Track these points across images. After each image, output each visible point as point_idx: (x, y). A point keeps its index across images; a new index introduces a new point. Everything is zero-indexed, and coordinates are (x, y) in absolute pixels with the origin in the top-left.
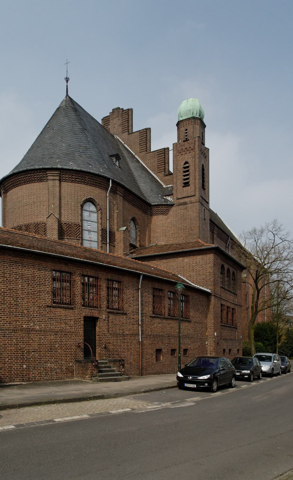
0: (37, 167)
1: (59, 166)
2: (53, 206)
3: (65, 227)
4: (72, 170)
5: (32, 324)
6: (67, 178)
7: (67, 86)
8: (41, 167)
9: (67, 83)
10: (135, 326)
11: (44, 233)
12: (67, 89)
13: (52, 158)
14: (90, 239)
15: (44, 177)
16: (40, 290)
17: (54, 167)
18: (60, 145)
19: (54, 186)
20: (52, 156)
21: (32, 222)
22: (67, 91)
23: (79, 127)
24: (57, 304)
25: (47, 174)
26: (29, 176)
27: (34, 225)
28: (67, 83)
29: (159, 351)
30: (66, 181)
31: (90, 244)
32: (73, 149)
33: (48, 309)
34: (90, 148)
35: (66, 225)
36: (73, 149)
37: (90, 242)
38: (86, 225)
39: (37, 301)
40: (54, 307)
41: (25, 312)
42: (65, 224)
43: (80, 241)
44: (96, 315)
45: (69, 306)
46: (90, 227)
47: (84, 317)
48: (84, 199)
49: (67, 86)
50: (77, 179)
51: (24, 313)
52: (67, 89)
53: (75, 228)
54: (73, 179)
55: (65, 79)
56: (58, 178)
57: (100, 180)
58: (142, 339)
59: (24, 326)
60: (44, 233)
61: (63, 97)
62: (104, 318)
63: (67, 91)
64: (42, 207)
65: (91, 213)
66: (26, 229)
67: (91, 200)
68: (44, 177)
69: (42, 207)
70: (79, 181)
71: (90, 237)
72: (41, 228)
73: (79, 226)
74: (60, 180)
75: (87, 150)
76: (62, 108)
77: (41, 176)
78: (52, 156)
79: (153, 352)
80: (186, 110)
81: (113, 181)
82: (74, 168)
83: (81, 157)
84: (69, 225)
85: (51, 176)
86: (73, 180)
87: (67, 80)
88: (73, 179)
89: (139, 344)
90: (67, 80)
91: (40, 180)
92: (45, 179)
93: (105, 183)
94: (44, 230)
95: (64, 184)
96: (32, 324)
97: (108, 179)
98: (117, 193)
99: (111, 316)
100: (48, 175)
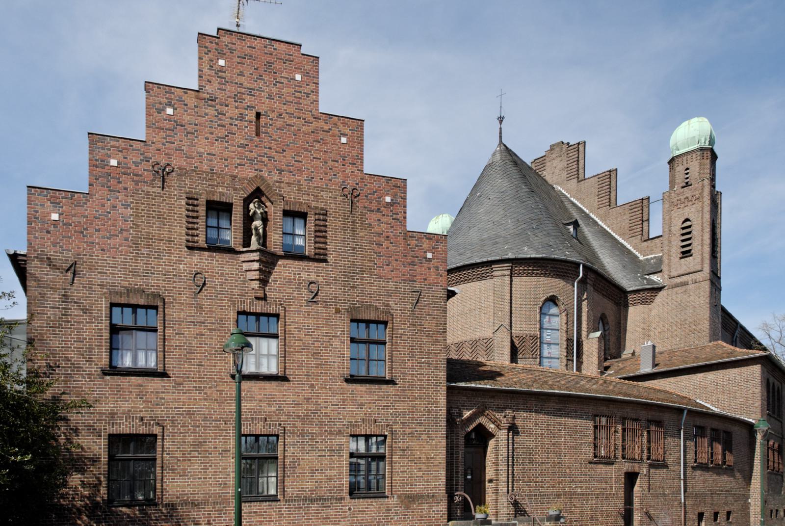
0: (479, 261)
1: (511, 255)
2: (500, 313)
3: (516, 342)
4: (530, 259)
5: (574, 486)
6: (521, 271)
7: (501, 128)
8: (485, 260)
9: (501, 124)
10: (676, 481)
11: (485, 353)
12: (501, 133)
13: (496, 243)
14: (549, 356)
15: (488, 273)
16: (581, 443)
17: (504, 257)
18: (503, 222)
19: (502, 286)
20: (495, 241)
21: (468, 338)
22: (501, 137)
23: (525, 190)
24: (598, 460)
25: (492, 269)
26: (465, 274)
27: (471, 342)
28: (501, 124)
29: (701, 516)
30: (519, 275)
31: (549, 362)
32: (523, 226)
33: (589, 466)
34: (545, 219)
35: (518, 339)
36: (523, 226)
37: (550, 360)
38: (547, 338)
39: (578, 456)
40: (595, 463)
41: (568, 471)
42: (516, 337)
43: (538, 360)
44: (637, 470)
45: (608, 462)
46: (549, 337)
47: (625, 473)
48: (545, 298)
49: (501, 128)
50: (534, 270)
51: (566, 473)
52: (501, 133)
53: (531, 342)
54: (530, 271)
55: (498, 119)
56: (508, 272)
57: (567, 268)
58: (685, 499)
59: (566, 489)
60: (485, 353)
61: (494, 145)
62: (645, 473)
63: (501, 137)
64: (482, 316)
65: (551, 317)
66: (456, 349)
67: (553, 300)
68: (488, 273)
69: (482, 316)
70: (538, 273)
71: (549, 353)
72: (481, 346)
73: (537, 339)
74: (511, 276)
75: (541, 224)
76: (497, 164)
77: (483, 272)
78: (495, 241)
79: (695, 517)
80: (686, 138)
81: (584, 266)
82: (533, 256)
83: (537, 236)
84: (522, 339)
85: (497, 271)
86: (529, 273)
87: (501, 119)
88: (530, 271)
89: (681, 507)
90: (501, 119)
91: (482, 278)
92: (488, 276)
93: (573, 271)
94: (485, 349)
95: (516, 280)
96: (574, 486)
97: (578, 265)
98: (587, 283)
99: (652, 471)
100: (494, 269)
